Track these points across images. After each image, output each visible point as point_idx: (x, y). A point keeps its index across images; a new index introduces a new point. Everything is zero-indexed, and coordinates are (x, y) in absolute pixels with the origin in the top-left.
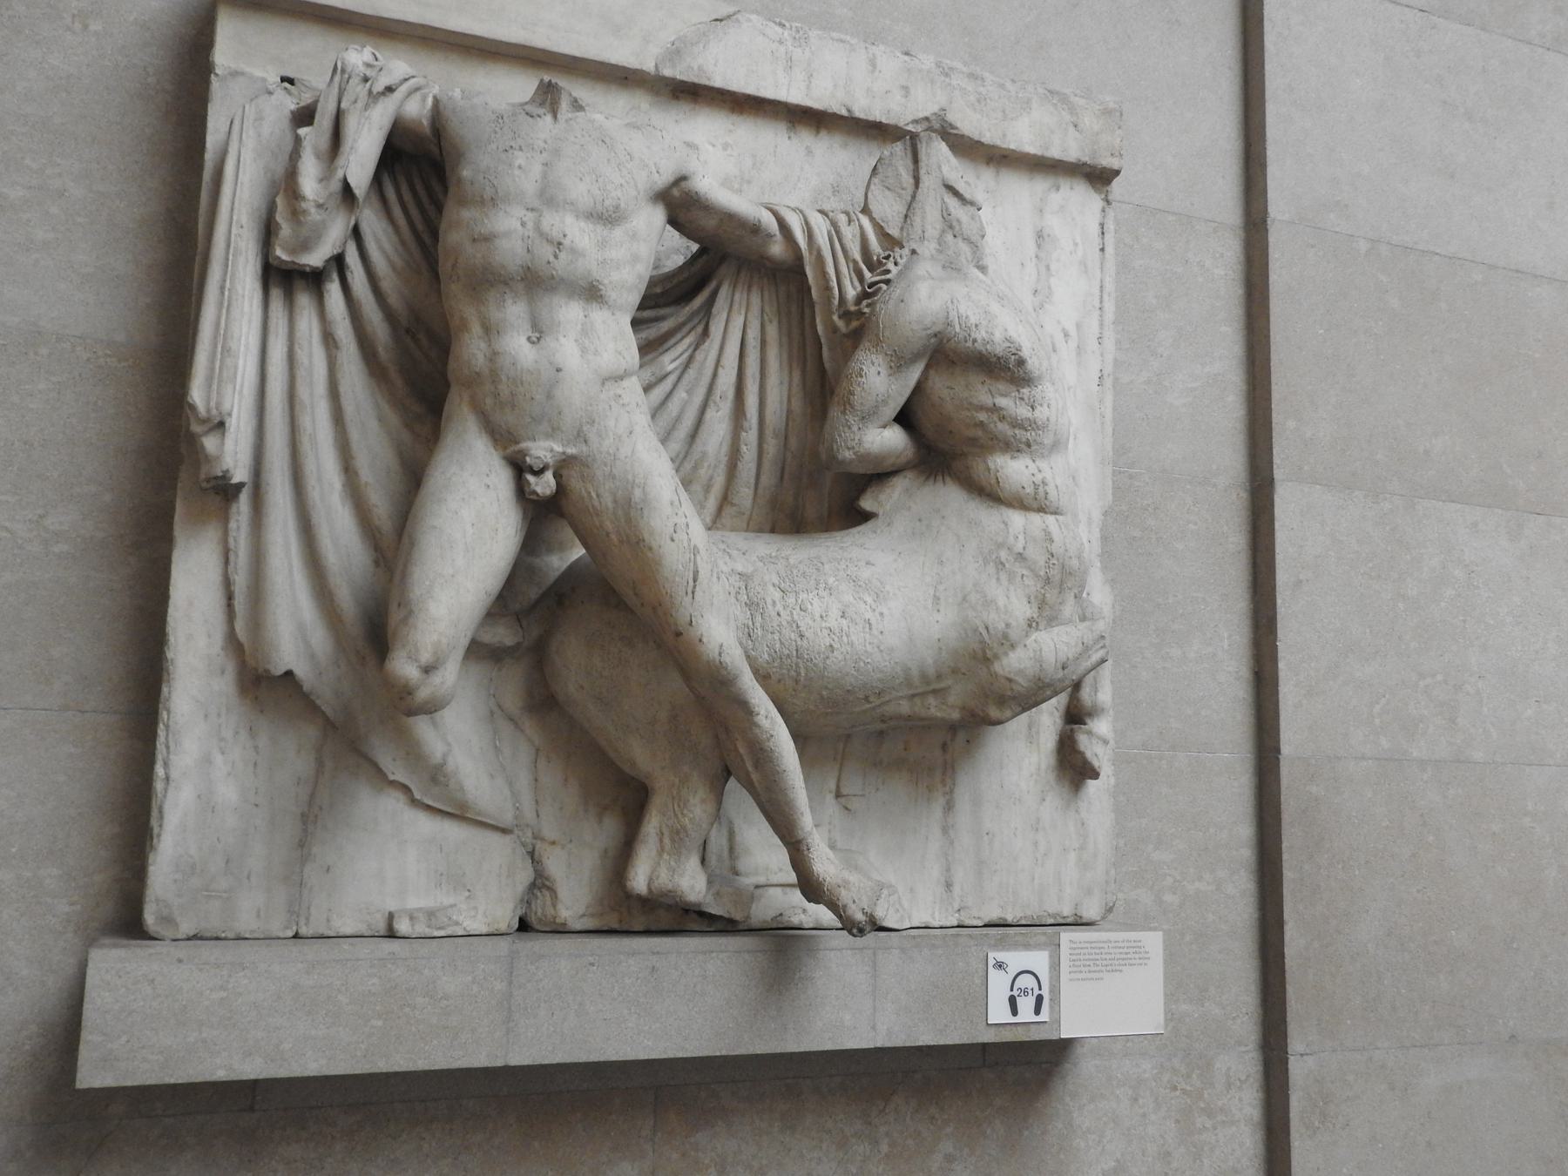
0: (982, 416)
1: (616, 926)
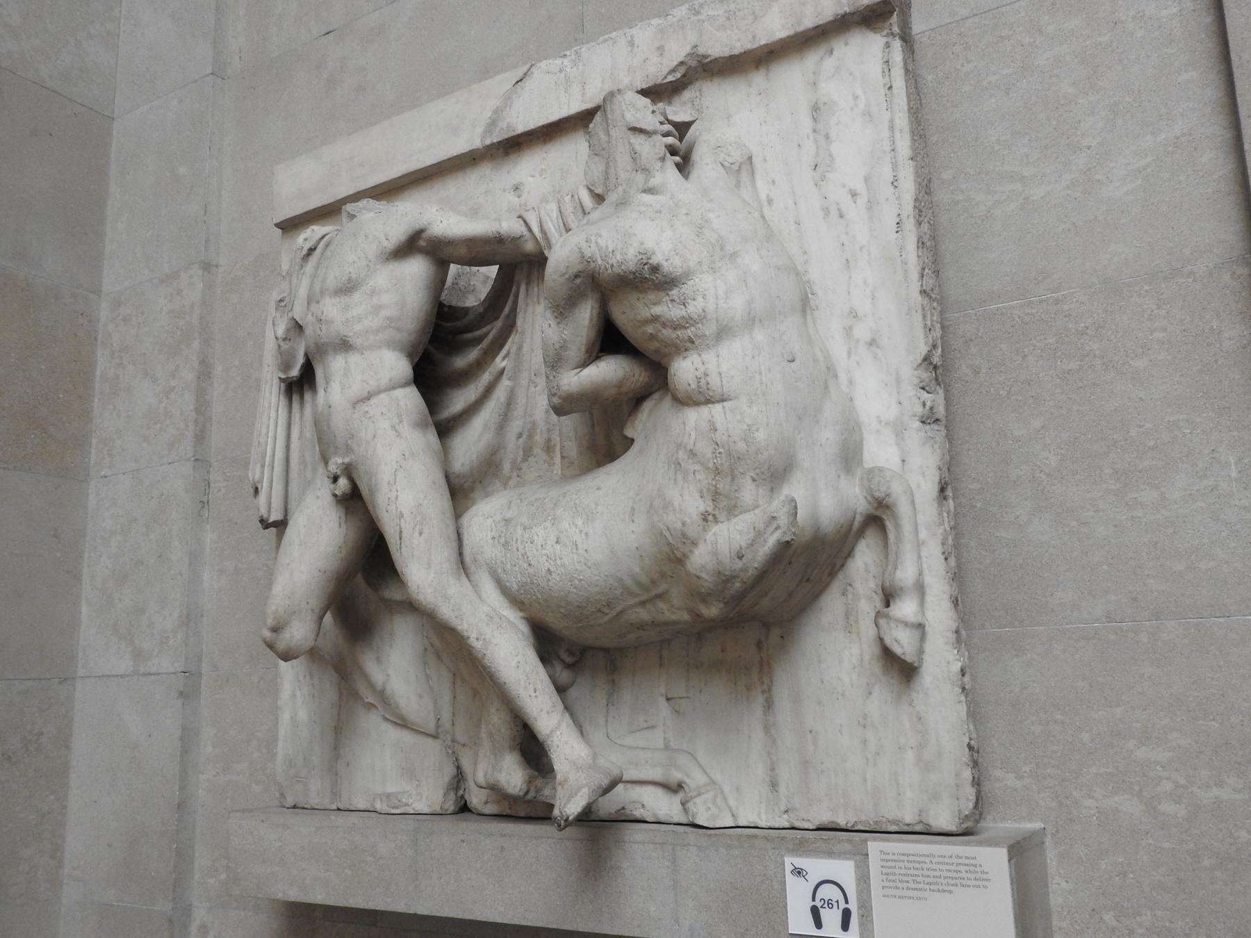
0: (650, 329)
1: (509, 812)
